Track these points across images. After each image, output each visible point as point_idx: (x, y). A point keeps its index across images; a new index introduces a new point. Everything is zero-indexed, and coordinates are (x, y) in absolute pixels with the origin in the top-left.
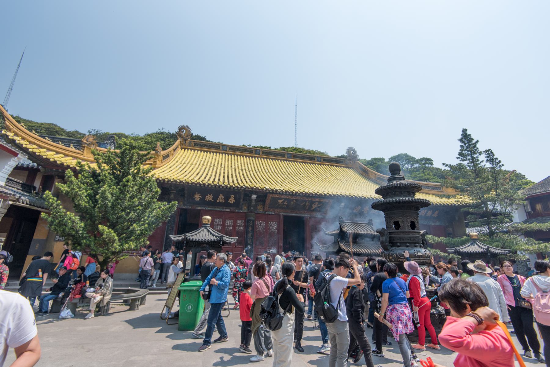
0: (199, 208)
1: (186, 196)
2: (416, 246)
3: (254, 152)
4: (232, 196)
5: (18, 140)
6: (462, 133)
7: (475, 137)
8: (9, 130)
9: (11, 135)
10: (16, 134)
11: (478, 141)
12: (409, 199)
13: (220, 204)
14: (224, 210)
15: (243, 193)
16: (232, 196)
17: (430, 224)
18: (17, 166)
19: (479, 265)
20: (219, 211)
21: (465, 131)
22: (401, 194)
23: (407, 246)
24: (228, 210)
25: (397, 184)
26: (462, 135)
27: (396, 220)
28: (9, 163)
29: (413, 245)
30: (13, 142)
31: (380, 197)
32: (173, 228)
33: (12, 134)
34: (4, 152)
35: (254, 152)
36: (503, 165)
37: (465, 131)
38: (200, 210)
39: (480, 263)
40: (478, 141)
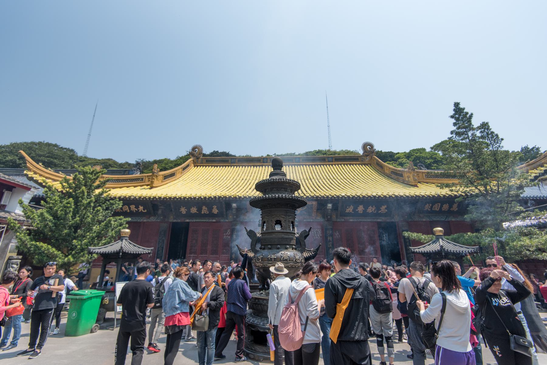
0: (188, 221)
1: (173, 210)
2: (286, 249)
3: (262, 160)
4: (215, 207)
5: (37, 177)
6: (454, 108)
7: (468, 110)
8: (30, 170)
9: (30, 174)
10: (35, 173)
11: (472, 114)
12: (279, 196)
13: (205, 216)
14: (211, 220)
15: (223, 203)
16: (215, 207)
17: (450, 219)
18: (33, 198)
19: (279, 267)
20: (206, 222)
21: (457, 105)
22: (278, 190)
23: (278, 248)
24: (214, 221)
25: (276, 179)
26: (454, 110)
27: (278, 219)
28: (25, 196)
29: (284, 246)
30: (31, 179)
31: (258, 194)
32: (163, 241)
33: (32, 173)
34: (21, 189)
35: (262, 160)
36: (502, 139)
37: (457, 105)
38: (188, 223)
39: (280, 265)
40: (472, 114)
